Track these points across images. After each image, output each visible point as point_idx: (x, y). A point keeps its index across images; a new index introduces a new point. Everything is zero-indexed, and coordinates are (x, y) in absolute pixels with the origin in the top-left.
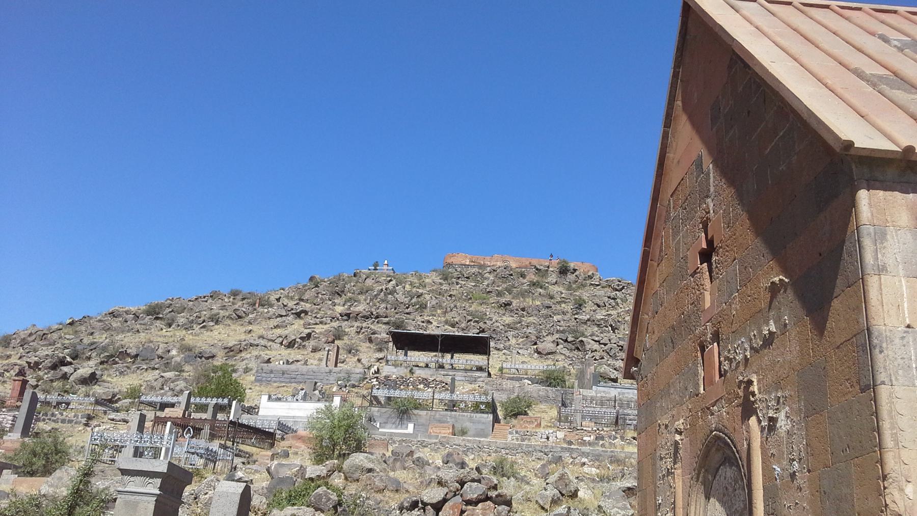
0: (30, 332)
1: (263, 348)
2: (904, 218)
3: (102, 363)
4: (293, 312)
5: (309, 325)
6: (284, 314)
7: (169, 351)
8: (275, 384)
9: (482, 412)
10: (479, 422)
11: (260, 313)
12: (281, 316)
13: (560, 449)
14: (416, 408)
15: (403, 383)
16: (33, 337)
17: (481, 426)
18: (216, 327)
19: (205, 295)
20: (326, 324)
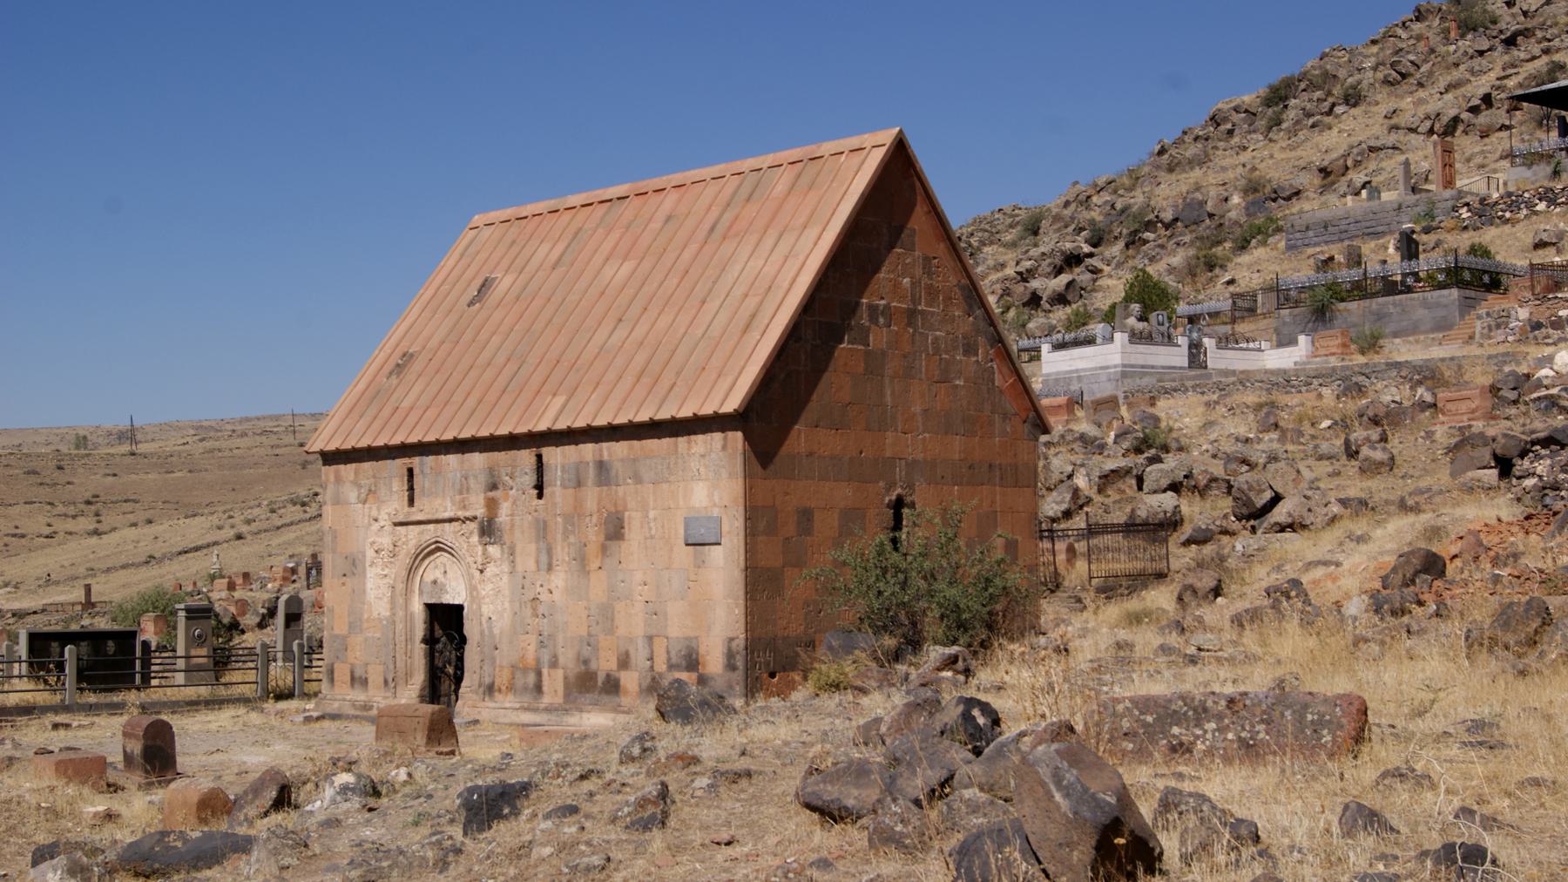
0: (1064, 199)
1: (1390, 151)
2: (332, 478)
3: (1127, 246)
4: (1503, 37)
5: (1514, 66)
6: (1485, 48)
7: (1226, 200)
8: (1310, 251)
9: (1442, 286)
10: (1438, 305)
11: (1439, 59)
12: (1481, 53)
13: (1384, 367)
14: (1343, 300)
15: (1510, 206)
16: (1073, 206)
17: (1440, 313)
18: (1354, 111)
19: (1403, 19)
20: (1558, 50)
